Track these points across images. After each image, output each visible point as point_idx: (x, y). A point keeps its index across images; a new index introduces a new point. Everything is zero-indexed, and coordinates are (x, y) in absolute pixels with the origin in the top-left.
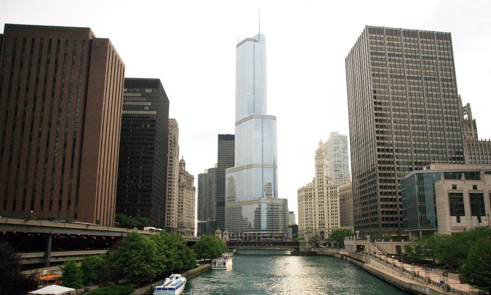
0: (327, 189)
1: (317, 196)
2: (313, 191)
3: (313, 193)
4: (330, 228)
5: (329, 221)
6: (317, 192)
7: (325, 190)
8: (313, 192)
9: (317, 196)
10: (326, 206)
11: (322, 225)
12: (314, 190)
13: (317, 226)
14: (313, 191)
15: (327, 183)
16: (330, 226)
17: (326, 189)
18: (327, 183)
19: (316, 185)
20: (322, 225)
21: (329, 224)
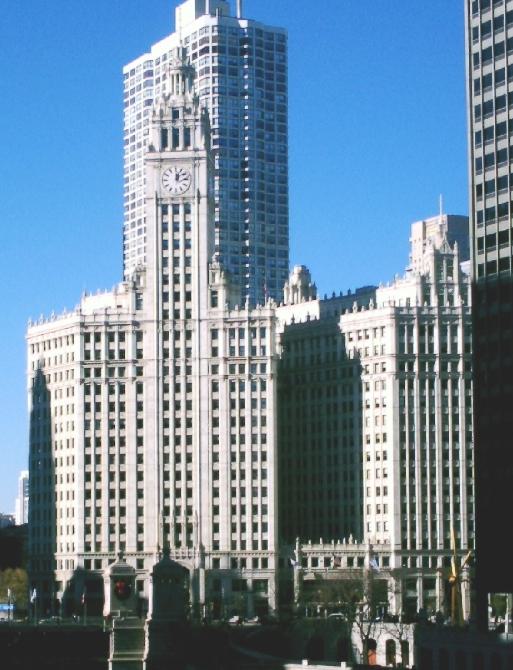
0: (214, 334)
1: (150, 369)
2: (130, 338)
3: (130, 355)
4: (224, 546)
5: (216, 510)
6: (150, 345)
7: (200, 343)
8: (129, 345)
9: (150, 369)
10: (201, 431)
11: (177, 528)
12: (139, 336)
13: (152, 538)
14: (130, 338)
15: (214, 303)
16: (223, 537)
17: (206, 335)
18: (214, 303)
19: (150, 310)
20: (177, 528)
21: (216, 528)
